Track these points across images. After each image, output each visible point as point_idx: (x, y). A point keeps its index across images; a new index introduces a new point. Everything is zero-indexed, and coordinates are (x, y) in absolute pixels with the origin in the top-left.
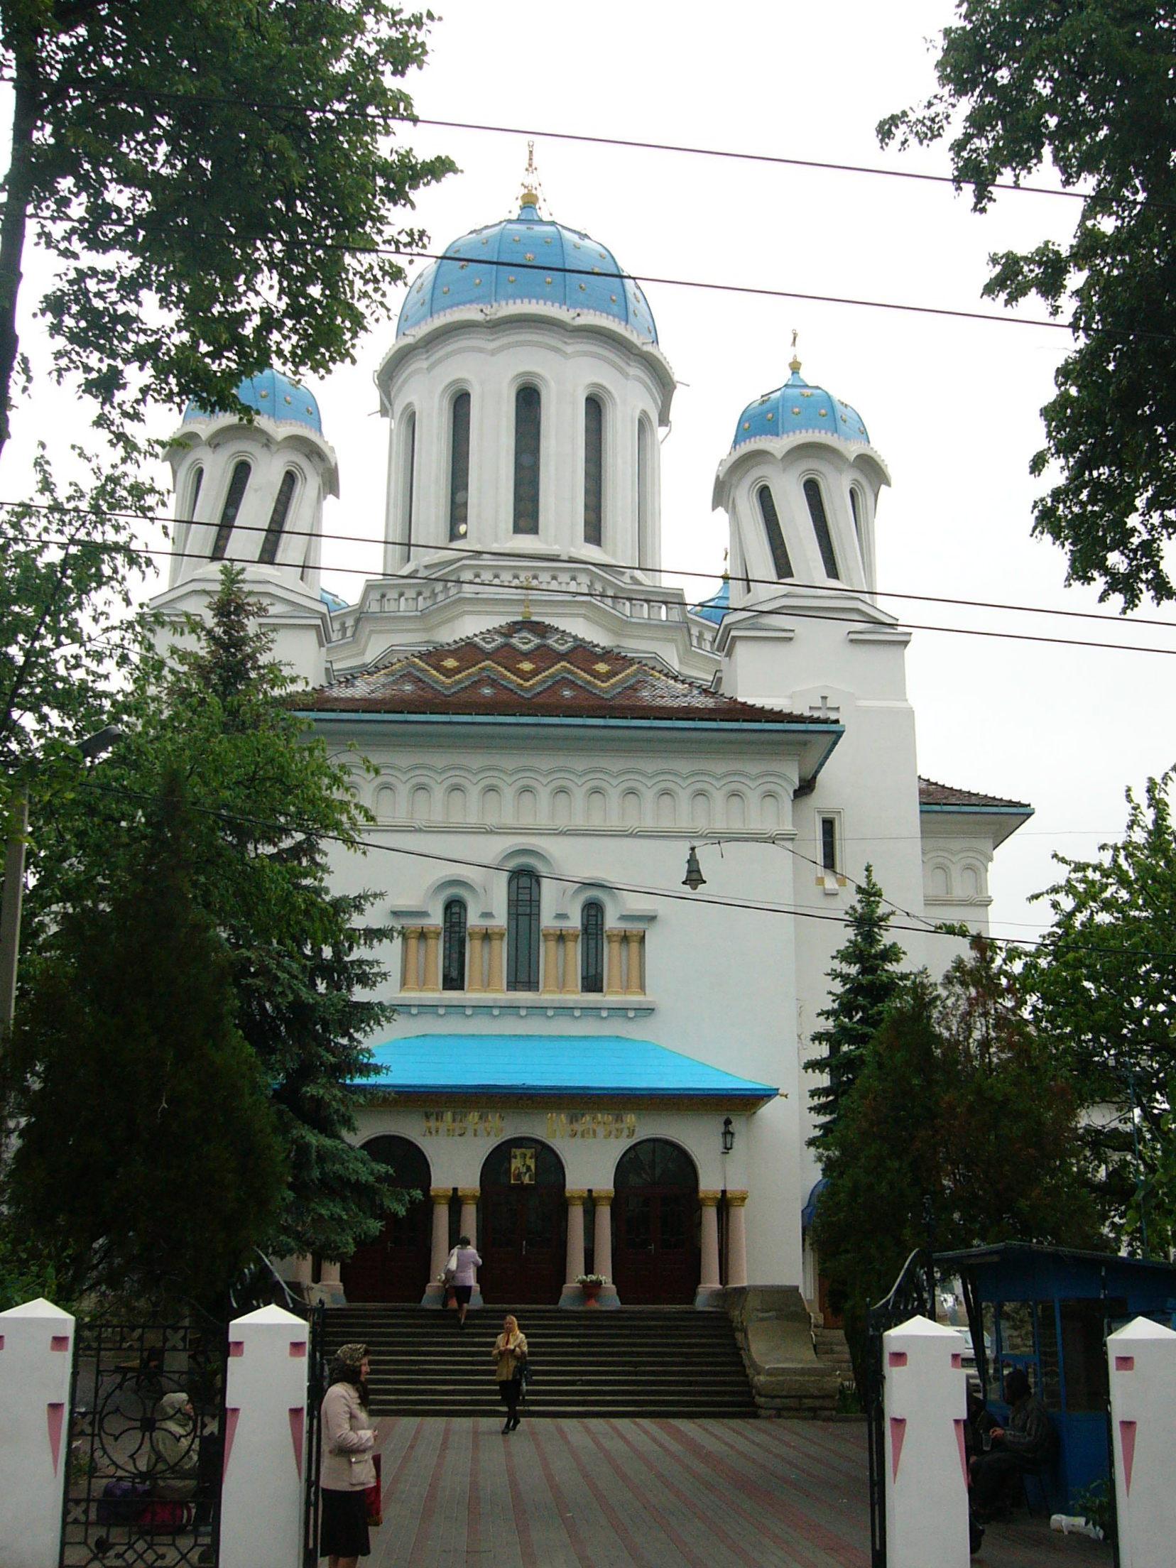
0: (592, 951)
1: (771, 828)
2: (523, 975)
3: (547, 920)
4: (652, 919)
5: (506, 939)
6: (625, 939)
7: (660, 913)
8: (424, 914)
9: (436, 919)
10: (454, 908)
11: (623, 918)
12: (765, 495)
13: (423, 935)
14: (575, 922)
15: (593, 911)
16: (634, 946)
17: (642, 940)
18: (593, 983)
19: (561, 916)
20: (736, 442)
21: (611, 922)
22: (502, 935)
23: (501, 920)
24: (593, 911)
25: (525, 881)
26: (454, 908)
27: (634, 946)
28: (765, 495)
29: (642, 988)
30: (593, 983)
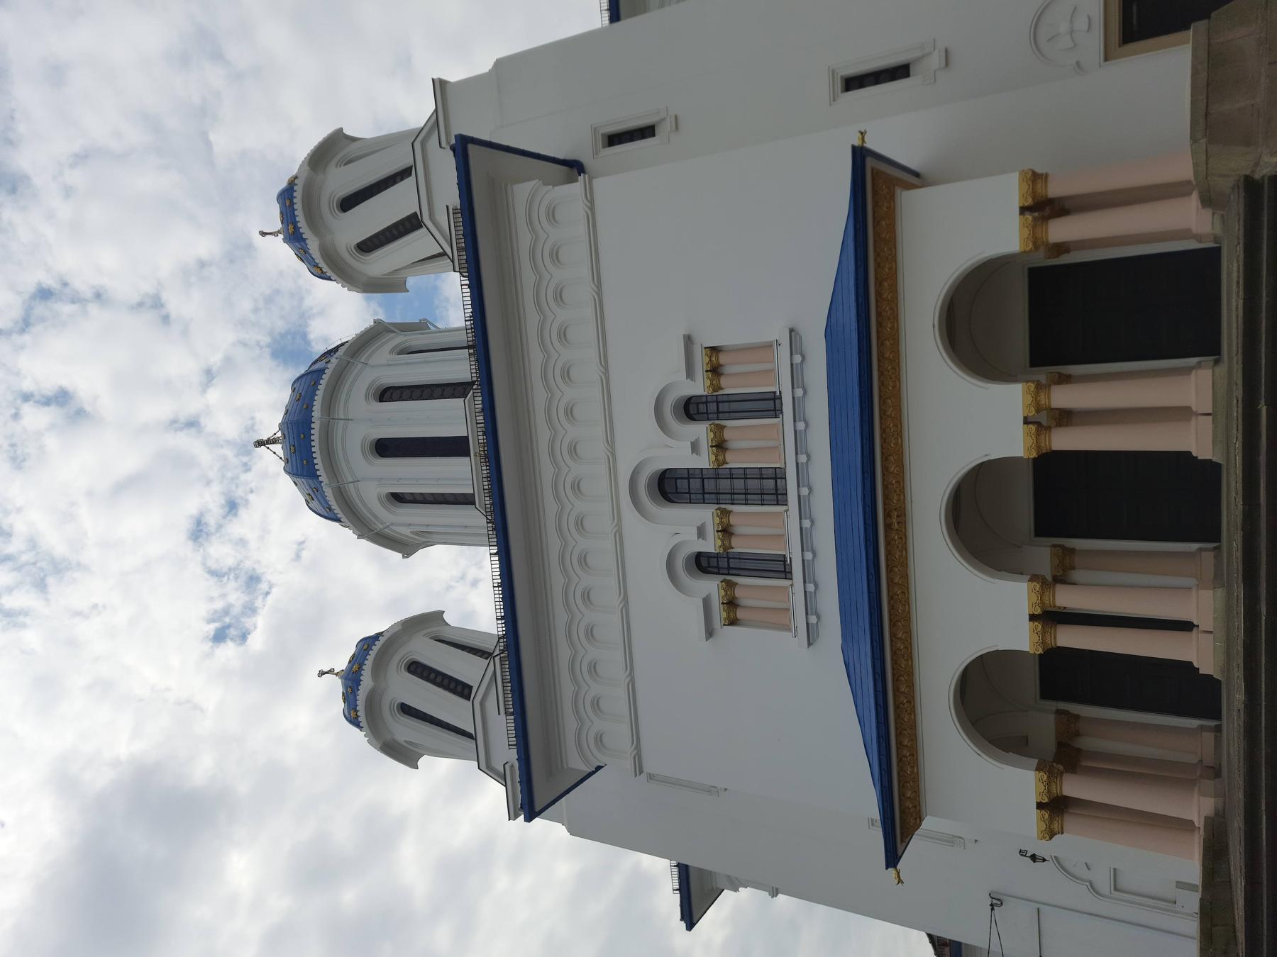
0: (734, 406)
1: (580, 208)
2: (768, 487)
3: (704, 461)
4: (688, 340)
5: (729, 507)
6: (715, 371)
7: (683, 332)
8: (707, 602)
9: (711, 586)
10: (702, 564)
11: (690, 374)
12: (367, 246)
13: (731, 603)
14: (701, 431)
15: (691, 409)
16: (723, 359)
17: (714, 350)
18: (769, 405)
19: (695, 447)
20: (329, 279)
21: (698, 387)
22: (725, 513)
23: (706, 514)
24: (691, 409)
25: (670, 486)
26: (702, 564)
27: (723, 359)
28: (367, 246)
29: (768, 346)
30: (769, 405)
